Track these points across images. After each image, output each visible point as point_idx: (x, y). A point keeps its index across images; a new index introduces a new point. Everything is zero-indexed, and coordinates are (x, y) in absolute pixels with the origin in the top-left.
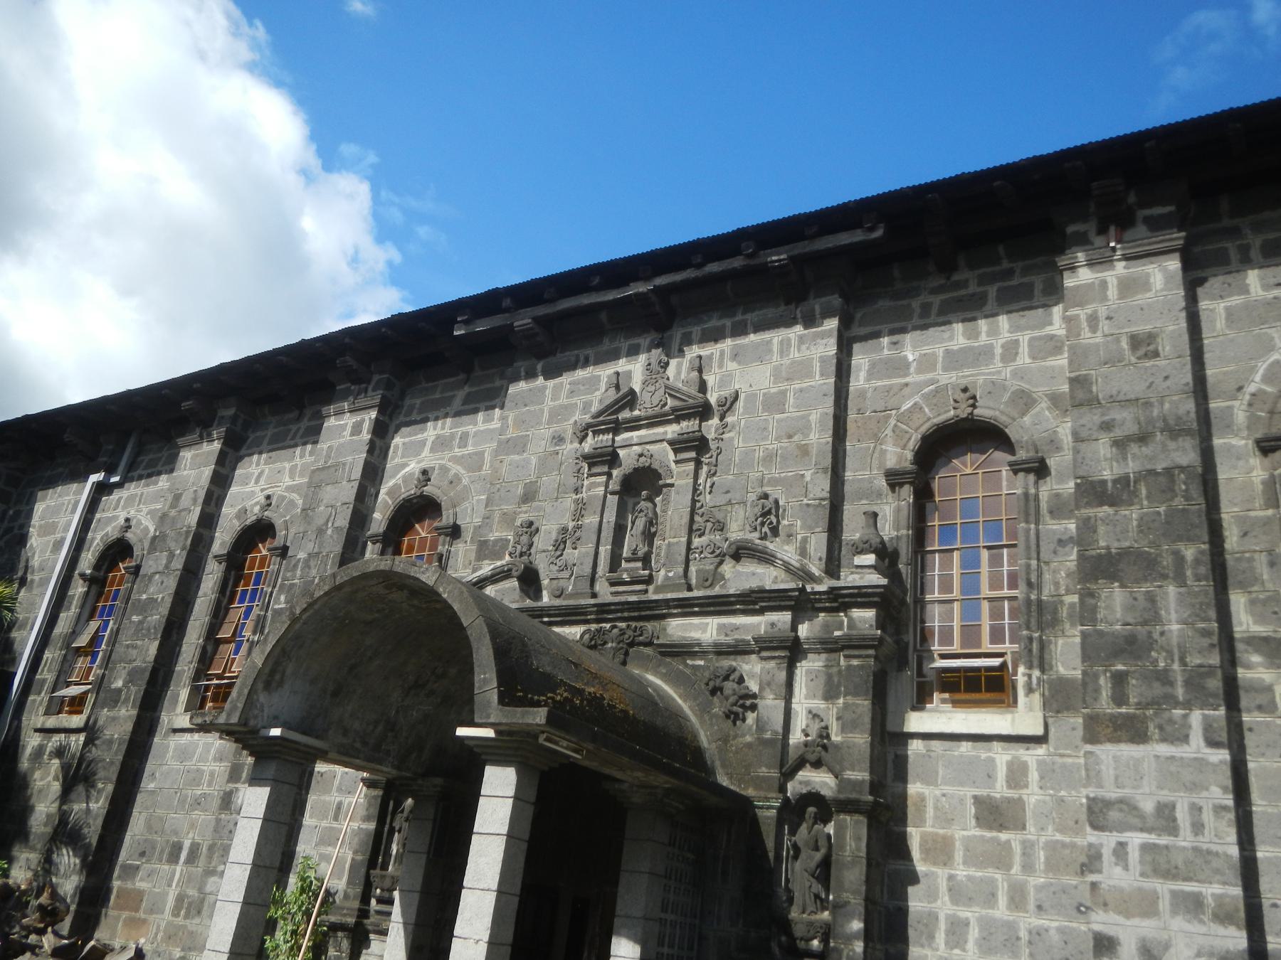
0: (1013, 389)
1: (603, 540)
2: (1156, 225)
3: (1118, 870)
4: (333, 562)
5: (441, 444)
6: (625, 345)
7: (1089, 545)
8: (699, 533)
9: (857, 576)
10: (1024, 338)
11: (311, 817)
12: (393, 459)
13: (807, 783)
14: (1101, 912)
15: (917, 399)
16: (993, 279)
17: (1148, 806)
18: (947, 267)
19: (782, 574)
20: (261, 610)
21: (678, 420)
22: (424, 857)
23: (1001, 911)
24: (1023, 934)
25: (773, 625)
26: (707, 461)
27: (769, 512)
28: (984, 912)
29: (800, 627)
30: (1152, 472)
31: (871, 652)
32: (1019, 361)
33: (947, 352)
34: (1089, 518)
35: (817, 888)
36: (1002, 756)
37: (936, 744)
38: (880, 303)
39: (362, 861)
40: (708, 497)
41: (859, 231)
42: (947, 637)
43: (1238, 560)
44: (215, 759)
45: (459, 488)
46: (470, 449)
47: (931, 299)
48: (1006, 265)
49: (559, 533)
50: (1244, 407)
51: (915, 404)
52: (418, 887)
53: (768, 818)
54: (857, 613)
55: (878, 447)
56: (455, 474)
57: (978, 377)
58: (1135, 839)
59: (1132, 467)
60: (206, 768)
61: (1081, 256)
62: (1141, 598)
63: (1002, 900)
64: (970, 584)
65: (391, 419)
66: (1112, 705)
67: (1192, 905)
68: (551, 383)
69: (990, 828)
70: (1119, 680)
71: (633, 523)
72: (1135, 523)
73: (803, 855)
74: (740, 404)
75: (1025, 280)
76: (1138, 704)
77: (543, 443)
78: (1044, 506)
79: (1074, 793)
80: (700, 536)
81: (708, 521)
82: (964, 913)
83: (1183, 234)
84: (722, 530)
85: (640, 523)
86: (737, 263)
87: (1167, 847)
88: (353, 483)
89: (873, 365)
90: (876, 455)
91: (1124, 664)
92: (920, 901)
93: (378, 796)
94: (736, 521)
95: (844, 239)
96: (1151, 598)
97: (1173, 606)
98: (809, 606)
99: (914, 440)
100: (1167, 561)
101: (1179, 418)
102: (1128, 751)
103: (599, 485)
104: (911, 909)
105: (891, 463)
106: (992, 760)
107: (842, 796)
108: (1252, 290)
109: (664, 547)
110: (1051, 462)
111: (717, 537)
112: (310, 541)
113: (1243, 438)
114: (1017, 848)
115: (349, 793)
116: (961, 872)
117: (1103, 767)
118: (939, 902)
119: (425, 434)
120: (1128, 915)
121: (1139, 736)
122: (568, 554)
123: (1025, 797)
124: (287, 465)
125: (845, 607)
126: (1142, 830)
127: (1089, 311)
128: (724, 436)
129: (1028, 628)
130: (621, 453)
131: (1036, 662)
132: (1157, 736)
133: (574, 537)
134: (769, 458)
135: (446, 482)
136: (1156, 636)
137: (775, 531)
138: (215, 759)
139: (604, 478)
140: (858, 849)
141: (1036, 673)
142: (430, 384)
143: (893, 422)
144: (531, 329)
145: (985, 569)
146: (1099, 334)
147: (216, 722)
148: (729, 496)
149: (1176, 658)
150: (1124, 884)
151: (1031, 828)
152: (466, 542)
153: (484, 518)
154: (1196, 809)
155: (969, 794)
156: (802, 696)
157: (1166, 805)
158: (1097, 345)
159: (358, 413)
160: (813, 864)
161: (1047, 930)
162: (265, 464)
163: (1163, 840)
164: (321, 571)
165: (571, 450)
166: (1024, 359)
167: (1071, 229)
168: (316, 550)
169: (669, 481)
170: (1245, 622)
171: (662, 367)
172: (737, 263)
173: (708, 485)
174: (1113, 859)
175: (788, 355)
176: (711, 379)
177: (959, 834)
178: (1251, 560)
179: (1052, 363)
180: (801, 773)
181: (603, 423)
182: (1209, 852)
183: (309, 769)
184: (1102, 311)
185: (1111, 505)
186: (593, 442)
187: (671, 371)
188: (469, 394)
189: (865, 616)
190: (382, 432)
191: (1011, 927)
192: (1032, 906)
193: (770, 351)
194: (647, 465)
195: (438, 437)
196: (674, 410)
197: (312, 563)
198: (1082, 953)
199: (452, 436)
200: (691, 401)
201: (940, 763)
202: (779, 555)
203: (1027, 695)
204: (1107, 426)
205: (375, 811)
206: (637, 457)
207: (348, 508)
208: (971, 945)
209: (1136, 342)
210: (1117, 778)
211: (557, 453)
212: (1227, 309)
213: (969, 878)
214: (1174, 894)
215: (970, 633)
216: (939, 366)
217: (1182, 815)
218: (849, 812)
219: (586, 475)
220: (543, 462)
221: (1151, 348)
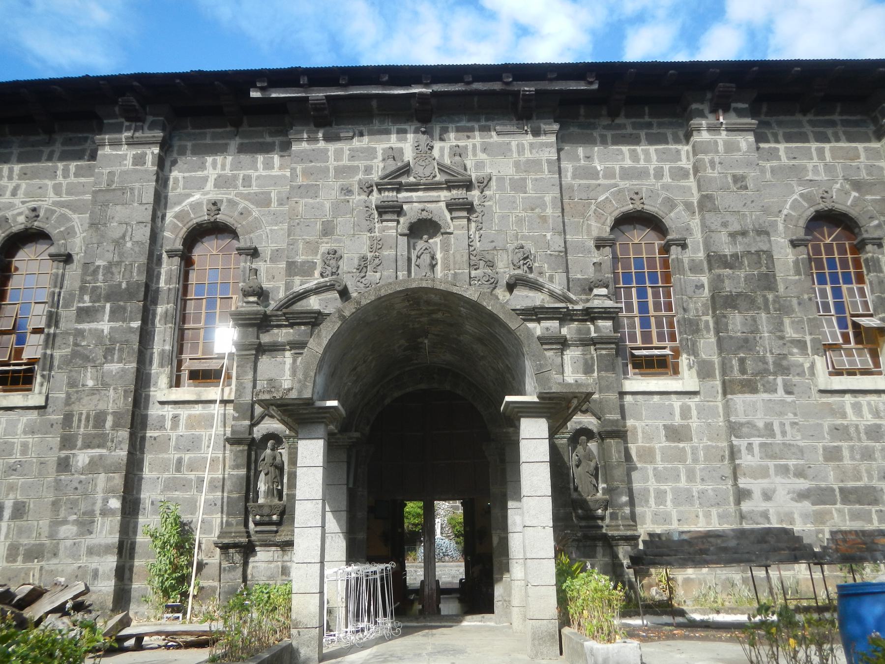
0: (663, 196)
1: (399, 268)
2: (740, 113)
3: (749, 457)
4: (139, 270)
5: (222, 182)
6: (394, 128)
7: (721, 289)
8: (475, 267)
9: (600, 302)
10: (666, 167)
11: (151, 471)
12: (174, 189)
13: (580, 423)
14: (743, 478)
15: (607, 194)
16: (641, 126)
17: (760, 424)
18: (613, 114)
19: (547, 298)
20: (52, 307)
21: (449, 188)
22: (345, 487)
23: (683, 483)
24: (695, 494)
25: (547, 329)
26: (475, 219)
27: (527, 257)
28: (674, 485)
29: (562, 330)
30: (749, 252)
31: (613, 346)
32: (665, 180)
33: (622, 168)
34: (720, 275)
35: (594, 481)
36: (677, 403)
37: (639, 398)
38: (572, 129)
39: (239, 497)
40: (478, 244)
41: (582, 83)
42: (633, 338)
43: (784, 300)
44: (25, 432)
45: (250, 219)
46: (254, 189)
47: (605, 132)
48: (647, 119)
49: (360, 260)
50: (782, 221)
51: (607, 198)
52: (344, 508)
53: (562, 444)
54: (600, 323)
55: (586, 222)
56: (244, 207)
57: (646, 185)
58: (756, 441)
59: (739, 249)
60: (16, 440)
61: (704, 122)
62: (749, 319)
63: (683, 478)
64: (643, 307)
65: (166, 154)
66: (740, 375)
67: (784, 470)
68: (332, 147)
69: (674, 441)
70: (742, 361)
71: (418, 257)
72: (743, 279)
73: (583, 464)
74: (493, 183)
75: (661, 131)
76: (752, 374)
77: (334, 192)
78: (686, 266)
79: (715, 420)
80: (476, 269)
81: (481, 260)
82: (663, 487)
83: (754, 121)
84: (492, 266)
85: (426, 258)
86: (497, 86)
87: (771, 444)
88: (147, 206)
89: (575, 169)
90: (585, 227)
91: (744, 353)
92: (639, 483)
93: (242, 451)
94: (502, 261)
95: (573, 86)
96: (754, 320)
97: (765, 323)
98: (569, 318)
99: (610, 221)
100: (760, 300)
101: (760, 224)
102: (749, 397)
103: (391, 228)
104: (634, 488)
105: (595, 233)
106: (672, 405)
107: (609, 429)
108: (782, 157)
109: (450, 275)
110: (688, 241)
112: (108, 251)
113: (783, 238)
115: (188, 451)
116: (660, 466)
117: (738, 406)
118: (650, 483)
119: (206, 172)
120: (755, 478)
121: (754, 390)
122: (370, 276)
123: (691, 424)
124: (50, 183)
125: (593, 320)
126: (759, 436)
127: (710, 157)
128: (485, 204)
129: (686, 334)
130: (405, 207)
131: (691, 352)
132: (762, 390)
133: (374, 264)
134: (520, 221)
135: (236, 214)
136: (758, 338)
137: (531, 269)
138: (25, 432)
139: (395, 224)
140: (620, 457)
141: (692, 358)
142: (197, 131)
143: (593, 207)
144: (323, 104)
145: (650, 299)
146: (716, 171)
147: (287, 397)
148: (494, 244)
149: (768, 350)
150: (752, 463)
151: (695, 440)
152: (265, 261)
153: (288, 245)
154: (782, 425)
155: (661, 424)
156: (570, 372)
157: (769, 424)
158: (715, 177)
159: (136, 146)
160: (592, 468)
162: (19, 179)
163: (769, 441)
164: (127, 276)
165: (359, 200)
166: (667, 179)
167: (694, 106)
168: (116, 259)
169: (448, 231)
170: (790, 332)
171: (429, 149)
172: (497, 86)
173: (477, 236)
174: (747, 452)
175: (524, 155)
176: (469, 163)
177: (657, 446)
178: (790, 301)
179: (684, 184)
180: (574, 417)
182: (790, 445)
183: (139, 435)
184: (717, 159)
185: (731, 268)
186: (379, 196)
187: (436, 153)
188: (242, 144)
189: (606, 325)
190: (161, 163)
191: (689, 491)
192: (698, 480)
193: (511, 150)
194: (430, 217)
195: (219, 176)
196: (447, 182)
197: (114, 270)
199: (235, 177)
200: (460, 177)
201: (643, 408)
202: (547, 286)
203: (689, 370)
204: (725, 225)
205: (244, 461)
206: (420, 211)
207: (145, 226)
208: (669, 503)
209: (736, 179)
210: (745, 411)
211: (348, 201)
212: (771, 167)
213: (665, 468)
214: (775, 465)
215: (647, 337)
216: (617, 176)
217: (776, 427)
218: (612, 437)
219: (376, 220)
220: (336, 208)
221: (744, 183)
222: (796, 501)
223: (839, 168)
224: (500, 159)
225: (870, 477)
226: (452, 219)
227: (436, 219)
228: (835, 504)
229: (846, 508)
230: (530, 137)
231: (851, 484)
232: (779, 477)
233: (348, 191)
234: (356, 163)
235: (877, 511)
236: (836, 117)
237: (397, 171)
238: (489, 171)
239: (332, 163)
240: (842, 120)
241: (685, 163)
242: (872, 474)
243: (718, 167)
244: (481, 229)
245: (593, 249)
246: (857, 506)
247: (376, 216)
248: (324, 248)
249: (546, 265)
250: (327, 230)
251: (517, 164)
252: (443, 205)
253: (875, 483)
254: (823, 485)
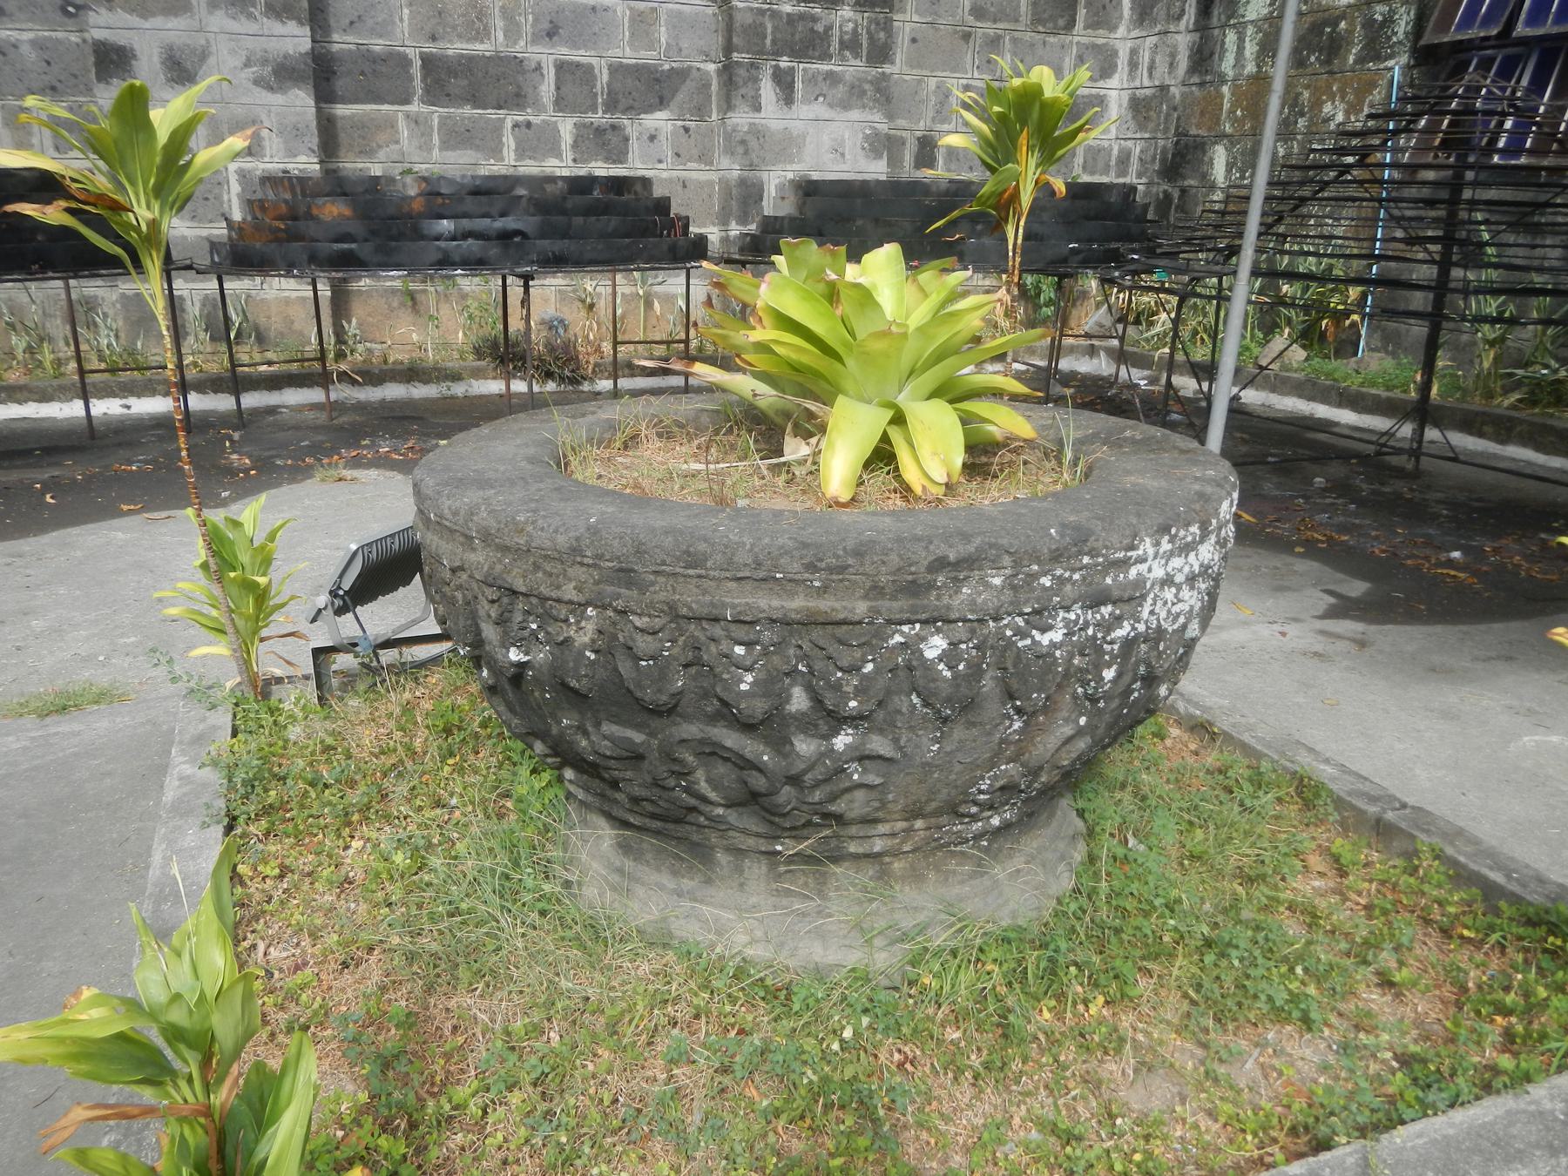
14: (103, 11)
161: (15, 46)
198: (75, 76)
222: (271, 89)
225: (512, 32)
228: (407, 101)
229: (436, 113)
231: (456, 48)
232: (220, 13)
235: (516, 125)
242: (518, 25)
246: (468, 111)
253: (520, 48)
254: (378, 45)
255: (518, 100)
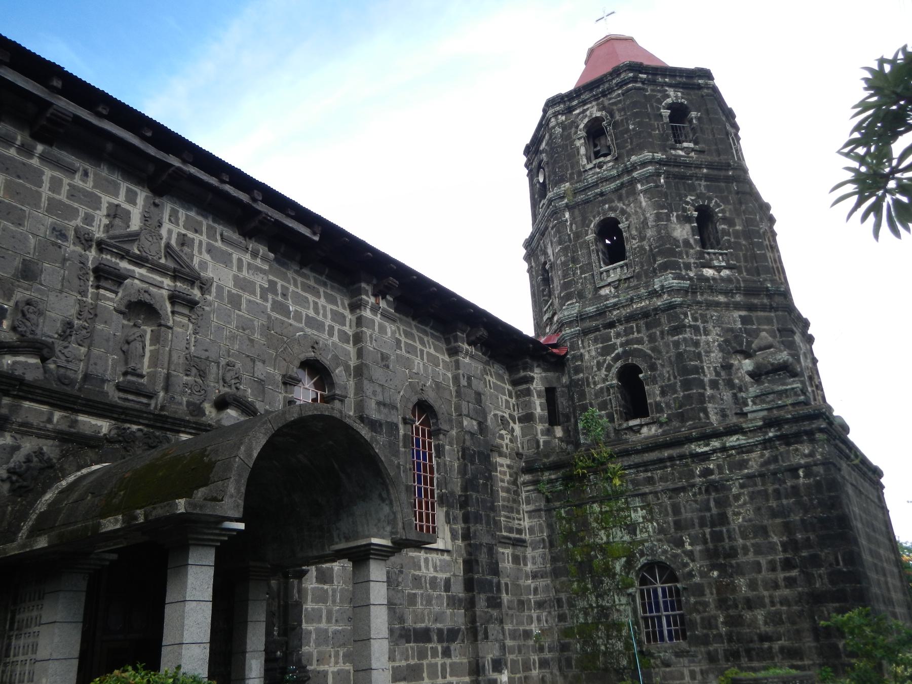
18: (303, 264)
23: (323, 625)
33: (307, 316)
40: (193, 348)
48: (323, 278)
63: (324, 620)
68: (48, 173)
86: (244, 197)
111: (199, 380)
114: (330, 593)
151: (335, 583)
165: (74, 251)
172: (244, 197)
181: (117, 247)
191: (326, 631)
192: (334, 621)
196: (175, 270)
211: (60, 247)
213: (313, 609)
219: (91, 283)
223: (430, 368)
224: (221, 266)
226: (173, 313)
227: (157, 307)
230: (247, 258)
233: (63, 236)
234: (76, 205)
236: (428, 329)
237: (127, 237)
238: (211, 275)
239: (45, 191)
240: (431, 333)
241: (349, 330)
243: (374, 343)
244: (197, 333)
245: (280, 384)
247: (92, 279)
248: (20, 295)
249: (249, 391)
250: (28, 273)
251: (236, 279)
252: (165, 293)
255: (429, 640)
